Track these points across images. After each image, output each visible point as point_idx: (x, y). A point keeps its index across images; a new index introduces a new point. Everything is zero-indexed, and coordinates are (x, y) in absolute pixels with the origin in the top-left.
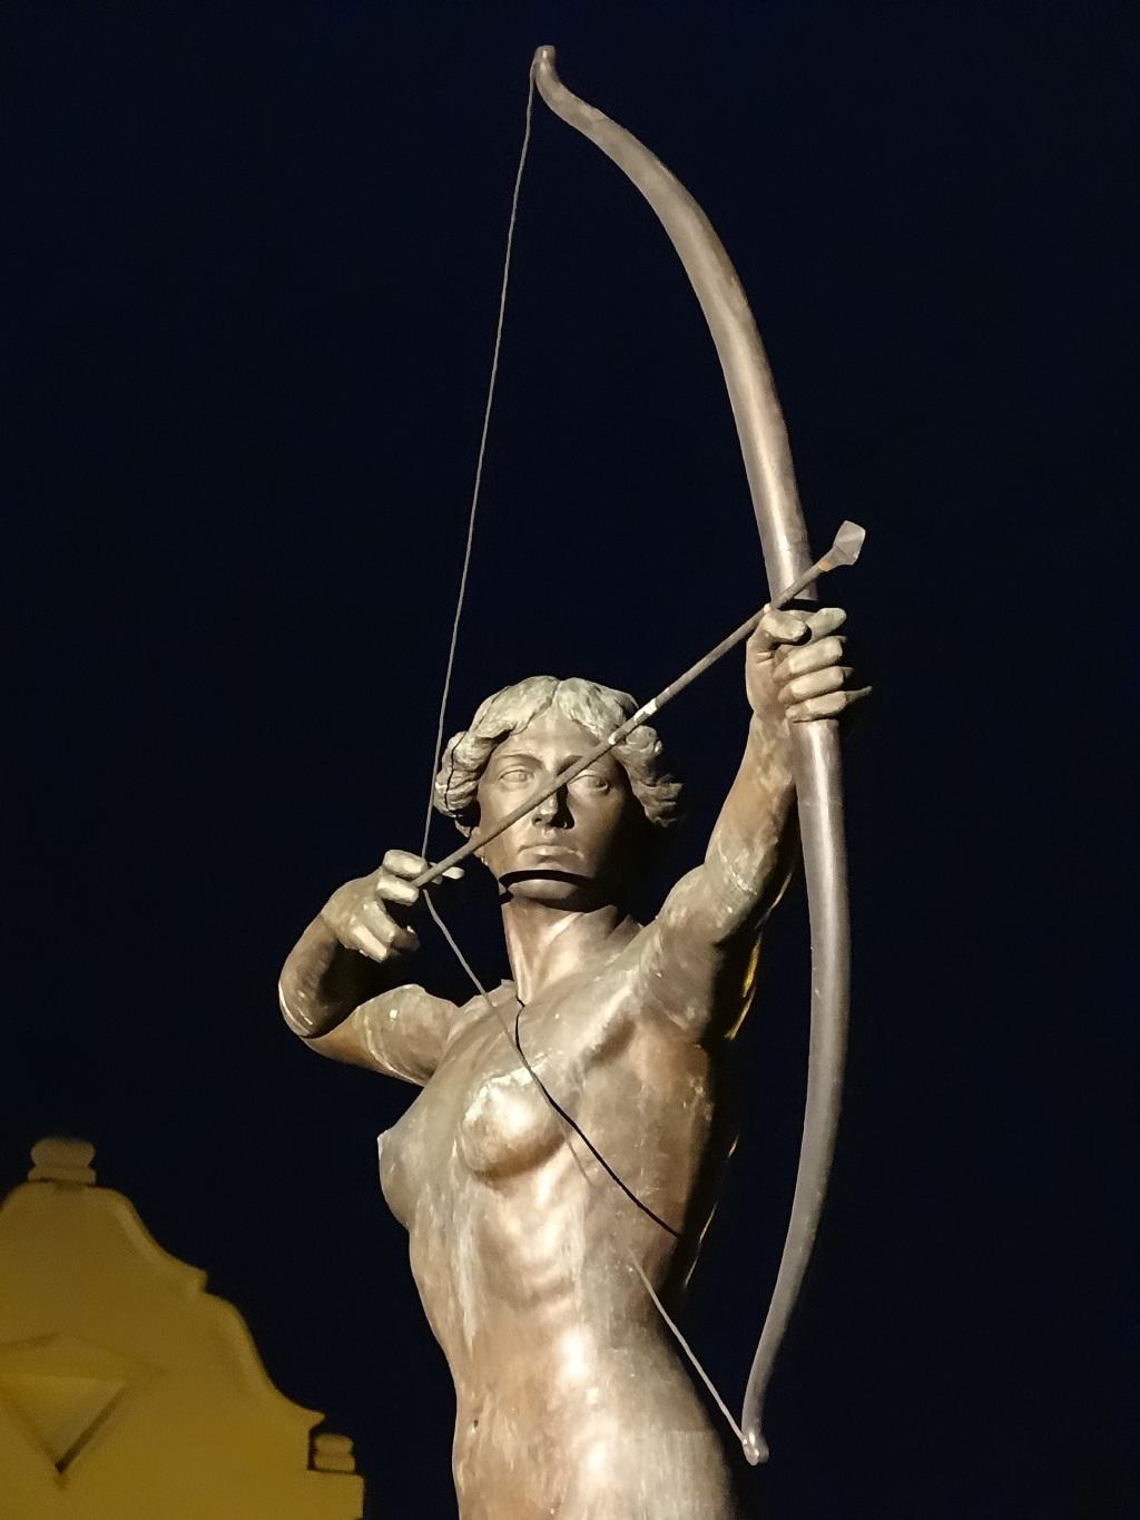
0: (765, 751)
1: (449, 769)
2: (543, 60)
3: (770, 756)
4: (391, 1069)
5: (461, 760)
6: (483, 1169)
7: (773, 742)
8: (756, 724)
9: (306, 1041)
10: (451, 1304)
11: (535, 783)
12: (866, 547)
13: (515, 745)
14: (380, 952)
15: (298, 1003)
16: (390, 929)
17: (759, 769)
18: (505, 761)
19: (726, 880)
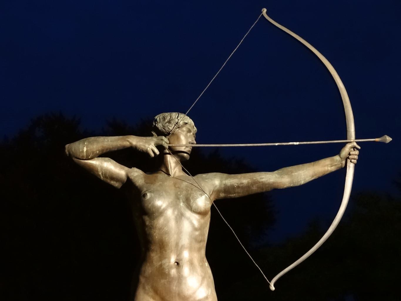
0: (336, 163)
1: (174, 125)
2: (265, 11)
3: (336, 165)
4: (100, 173)
5: (179, 124)
6: (198, 212)
7: (340, 163)
8: (337, 158)
9: (74, 159)
10: (175, 236)
11: (189, 134)
12: (391, 142)
13: (188, 126)
14: (152, 155)
15: (92, 154)
16: (157, 152)
17: (330, 166)
18: (184, 129)
19: (299, 180)
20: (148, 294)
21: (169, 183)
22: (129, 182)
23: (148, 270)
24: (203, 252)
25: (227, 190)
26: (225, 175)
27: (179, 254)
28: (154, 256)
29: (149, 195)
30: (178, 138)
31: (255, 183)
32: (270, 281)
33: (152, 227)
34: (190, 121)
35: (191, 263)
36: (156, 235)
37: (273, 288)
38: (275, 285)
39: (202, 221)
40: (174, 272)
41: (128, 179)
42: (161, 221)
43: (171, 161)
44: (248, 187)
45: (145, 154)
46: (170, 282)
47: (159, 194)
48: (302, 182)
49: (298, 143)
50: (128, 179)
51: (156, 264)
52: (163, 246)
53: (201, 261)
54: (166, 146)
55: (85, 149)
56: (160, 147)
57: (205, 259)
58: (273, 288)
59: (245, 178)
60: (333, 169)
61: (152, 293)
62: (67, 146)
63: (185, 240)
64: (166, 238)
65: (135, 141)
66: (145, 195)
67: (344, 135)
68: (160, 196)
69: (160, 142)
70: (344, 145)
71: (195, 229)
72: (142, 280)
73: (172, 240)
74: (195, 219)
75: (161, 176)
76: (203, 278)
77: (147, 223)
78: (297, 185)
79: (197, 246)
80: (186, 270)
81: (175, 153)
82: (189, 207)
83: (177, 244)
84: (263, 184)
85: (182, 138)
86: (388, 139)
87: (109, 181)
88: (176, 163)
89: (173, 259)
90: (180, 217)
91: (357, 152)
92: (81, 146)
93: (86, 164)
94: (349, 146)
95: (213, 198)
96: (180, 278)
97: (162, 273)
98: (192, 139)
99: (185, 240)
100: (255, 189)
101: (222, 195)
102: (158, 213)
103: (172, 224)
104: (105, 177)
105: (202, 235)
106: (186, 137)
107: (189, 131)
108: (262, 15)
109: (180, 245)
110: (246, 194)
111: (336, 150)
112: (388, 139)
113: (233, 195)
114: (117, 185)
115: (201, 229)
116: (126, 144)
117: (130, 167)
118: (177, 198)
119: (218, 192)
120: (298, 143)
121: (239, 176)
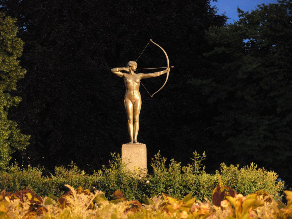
2: (151, 39)
8: (165, 71)
16: (129, 71)
21: (131, 77)
22: (124, 76)
23: (128, 94)
24: (138, 90)
25: (143, 77)
26: (143, 74)
27: (133, 91)
29: (127, 80)
30: (133, 67)
31: (149, 76)
32: (151, 95)
33: (128, 86)
35: (136, 93)
40: (132, 94)
41: (123, 75)
42: (130, 84)
44: (147, 76)
47: (129, 79)
50: (123, 75)
54: (131, 69)
56: (129, 70)
58: (152, 97)
62: (111, 70)
63: (135, 88)
64: (131, 88)
65: (125, 69)
66: (127, 80)
67: (166, 65)
68: (130, 80)
70: (166, 68)
71: (136, 86)
73: (132, 88)
74: (137, 84)
77: (127, 85)
80: (135, 94)
83: (133, 89)
85: (134, 67)
89: (132, 92)
90: (134, 83)
91: (170, 70)
94: (168, 68)
95: (140, 79)
96: (134, 95)
97: (131, 95)
98: (136, 67)
99: (135, 88)
100: (149, 77)
101: (143, 78)
102: (129, 83)
106: (135, 67)
108: (151, 41)
111: (165, 69)
114: (121, 77)
115: (138, 85)
116: (123, 69)
118: (133, 80)
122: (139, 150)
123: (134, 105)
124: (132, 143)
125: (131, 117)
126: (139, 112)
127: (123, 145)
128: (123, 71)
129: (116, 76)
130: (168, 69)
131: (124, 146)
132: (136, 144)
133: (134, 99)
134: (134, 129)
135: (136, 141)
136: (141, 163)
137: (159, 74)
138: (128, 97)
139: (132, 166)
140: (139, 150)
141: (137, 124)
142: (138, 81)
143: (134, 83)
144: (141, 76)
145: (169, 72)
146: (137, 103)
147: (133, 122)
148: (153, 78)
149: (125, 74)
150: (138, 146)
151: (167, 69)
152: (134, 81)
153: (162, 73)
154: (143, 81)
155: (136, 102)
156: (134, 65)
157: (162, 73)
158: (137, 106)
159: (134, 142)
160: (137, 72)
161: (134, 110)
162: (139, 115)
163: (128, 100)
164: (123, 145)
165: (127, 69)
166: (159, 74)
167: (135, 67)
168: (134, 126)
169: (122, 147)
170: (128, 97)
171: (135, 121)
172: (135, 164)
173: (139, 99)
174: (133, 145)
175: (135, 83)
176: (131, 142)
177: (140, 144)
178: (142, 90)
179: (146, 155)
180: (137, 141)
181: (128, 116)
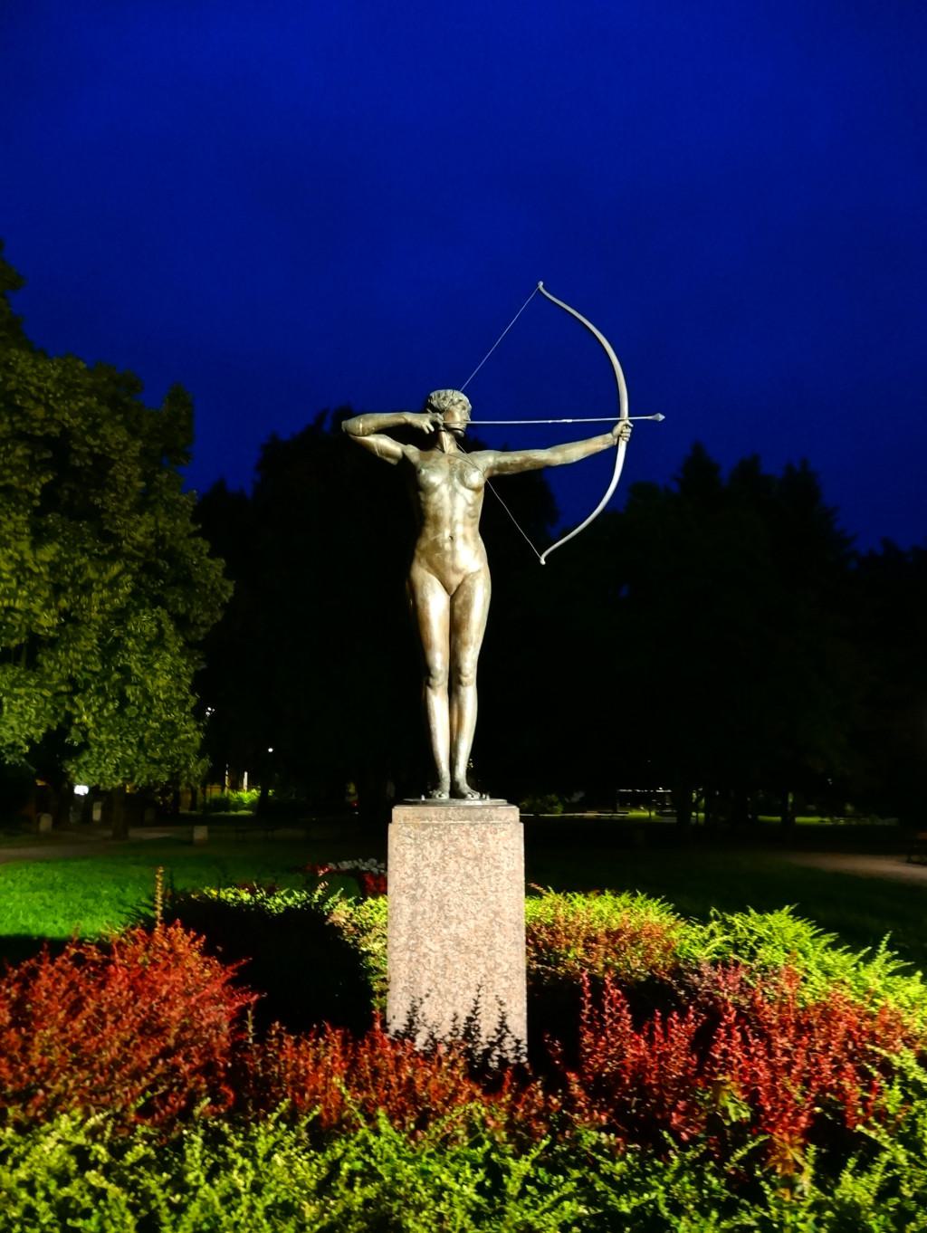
2: (541, 284)
8: (609, 436)
14: (427, 432)
16: (432, 429)
18: (459, 406)
20: (422, 566)
21: (443, 461)
22: (404, 459)
23: (423, 544)
24: (477, 527)
25: (500, 467)
26: (498, 453)
27: (453, 528)
28: (429, 530)
29: (424, 471)
30: (453, 415)
31: (527, 460)
33: (426, 503)
34: (465, 398)
35: (465, 537)
36: (431, 510)
37: (543, 562)
38: (545, 559)
39: (476, 497)
40: (447, 546)
41: (404, 455)
42: (435, 497)
43: (446, 438)
44: (521, 464)
45: (420, 430)
46: (444, 556)
48: (575, 460)
49: (570, 421)
50: (404, 455)
51: (431, 538)
52: (437, 521)
53: (475, 536)
54: (441, 423)
55: (361, 426)
56: (435, 424)
57: (478, 534)
58: (543, 562)
59: (518, 455)
60: (605, 447)
61: (427, 566)
62: (343, 423)
63: (459, 516)
64: (440, 514)
65: (410, 418)
66: (420, 472)
67: (618, 413)
69: (435, 419)
70: (617, 422)
72: (418, 553)
73: (446, 514)
74: (469, 495)
75: (436, 453)
76: (476, 552)
77: (422, 499)
78: (569, 462)
79: (470, 521)
80: (459, 544)
81: (450, 430)
82: (463, 483)
83: (451, 519)
84: (536, 461)
86: (661, 417)
87: (385, 458)
88: (451, 440)
89: (447, 533)
90: (454, 493)
91: (629, 430)
92: (357, 422)
93: (363, 441)
94: (621, 424)
95: (487, 475)
96: (453, 553)
97: (436, 546)
99: (459, 516)
100: (528, 466)
101: (496, 472)
103: (447, 500)
104: (381, 452)
105: (475, 510)
106: (460, 413)
107: (464, 408)
109: (454, 519)
110: (519, 471)
111: (608, 428)
112: (661, 417)
113: (506, 473)
114: (393, 461)
115: (474, 505)
116: (402, 420)
117: (406, 444)
118: (451, 474)
119: (492, 469)
120: (570, 421)
121: (513, 453)
122: (482, 839)
123: (453, 599)
124: (445, 796)
125: (439, 660)
126: (478, 632)
127: (399, 812)
128: (402, 433)
129: (366, 450)
130: (624, 425)
131: (402, 815)
132: (467, 803)
133: (457, 571)
134: (455, 722)
135: (464, 787)
136: (496, 914)
137: (575, 452)
138: (423, 560)
139: (445, 931)
140: (482, 839)
141: (470, 695)
142: (477, 478)
143: (454, 493)
144: (488, 460)
145: (629, 445)
146: (471, 590)
147: (446, 684)
148: (548, 469)
149: (412, 451)
150: (479, 814)
151: (617, 429)
152: (456, 480)
153: (598, 444)
154: (497, 486)
155: (468, 582)
156: (458, 408)
157: (598, 444)
158: (467, 605)
159: (456, 793)
160: (470, 442)
161: (456, 628)
162: (478, 652)
163: (426, 573)
164: (399, 812)
165: (424, 422)
166: (575, 452)
167: (460, 416)
168: (455, 706)
169: (388, 819)
170: (423, 560)
171: (460, 682)
172: (461, 916)
173: (479, 571)
174: (451, 811)
175: (462, 489)
176: (436, 794)
177: (488, 801)
178: (492, 527)
179: (523, 865)
180: (468, 784)
181: (429, 652)
